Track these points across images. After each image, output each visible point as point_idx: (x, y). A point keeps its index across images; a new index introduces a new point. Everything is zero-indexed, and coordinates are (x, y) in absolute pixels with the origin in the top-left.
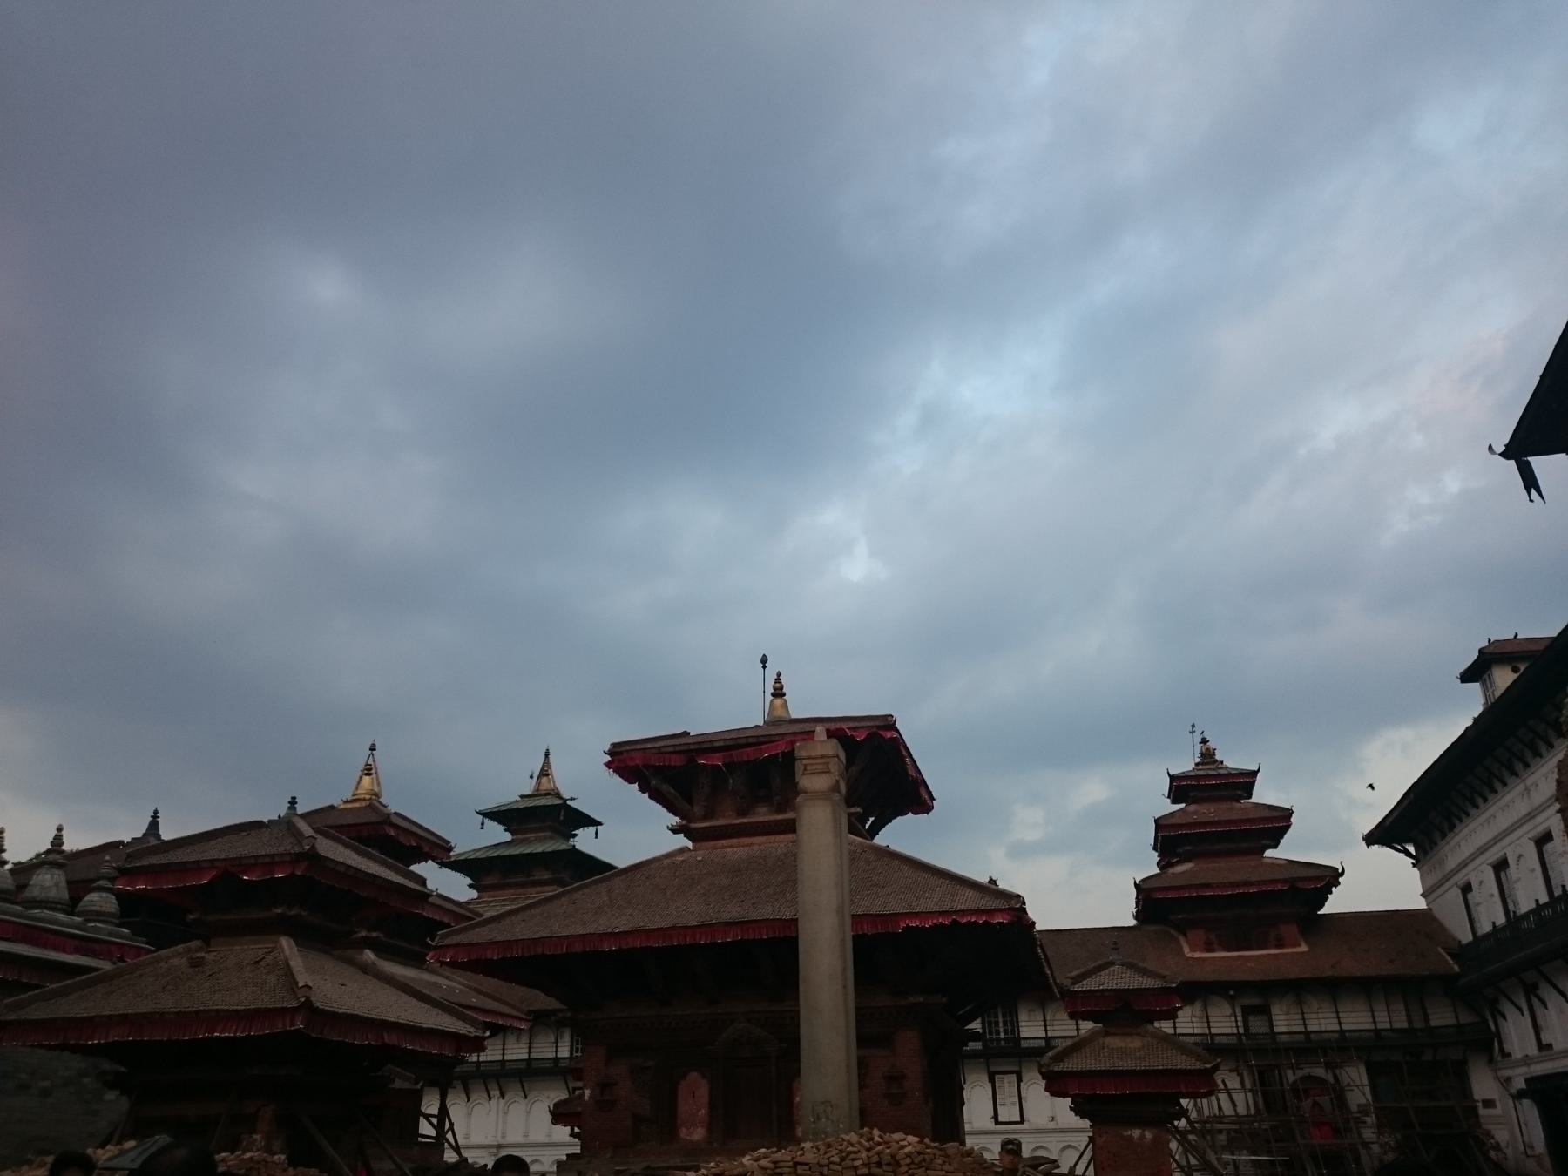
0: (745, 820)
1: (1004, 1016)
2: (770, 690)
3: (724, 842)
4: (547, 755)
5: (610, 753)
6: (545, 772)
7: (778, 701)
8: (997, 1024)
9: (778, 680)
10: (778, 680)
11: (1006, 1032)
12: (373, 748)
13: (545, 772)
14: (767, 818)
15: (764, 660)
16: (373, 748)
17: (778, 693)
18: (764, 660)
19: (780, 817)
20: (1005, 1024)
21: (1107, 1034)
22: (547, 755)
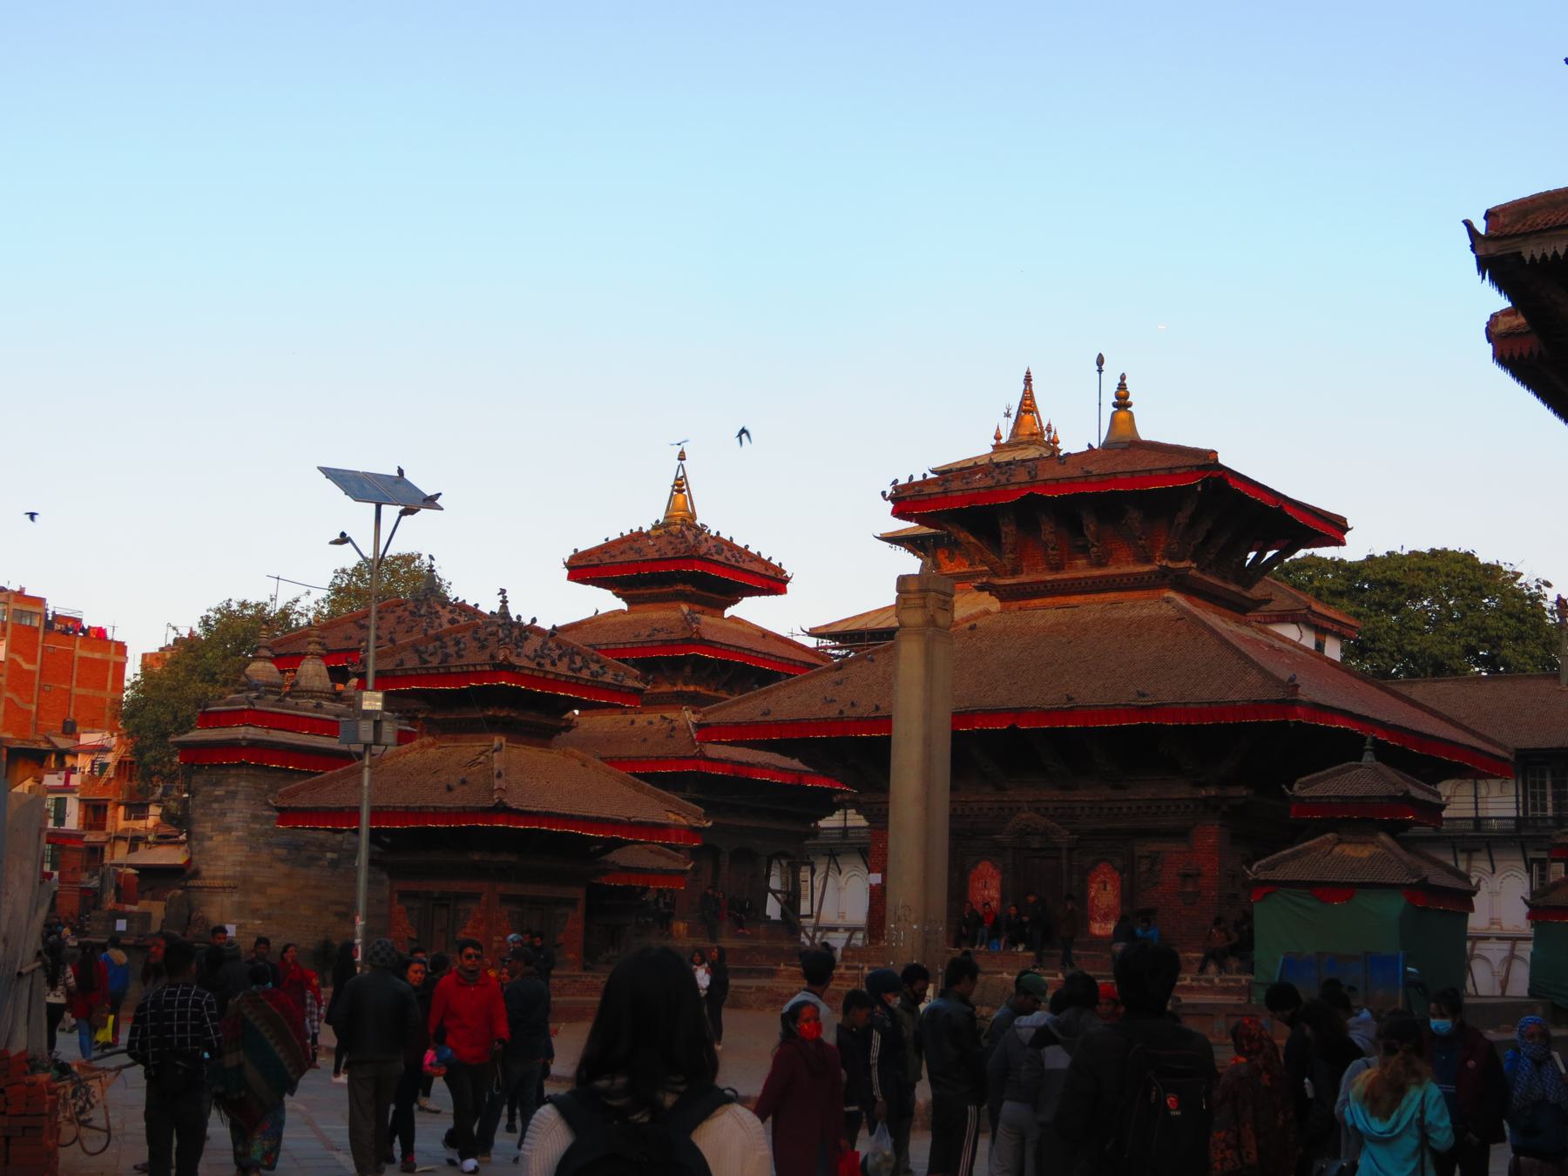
0: (1058, 576)
1: (1554, 785)
2: (1110, 398)
3: (1036, 602)
4: (1028, 379)
5: (893, 499)
6: (1028, 405)
7: (1122, 415)
8: (1544, 797)
9: (1122, 386)
10: (1122, 386)
11: (1556, 807)
12: (682, 457)
13: (1028, 405)
14: (1081, 574)
15: (1100, 361)
16: (682, 457)
17: (1122, 402)
18: (1100, 361)
19: (1097, 572)
20: (1554, 797)
21: (1340, 842)
22: (1028, 379)
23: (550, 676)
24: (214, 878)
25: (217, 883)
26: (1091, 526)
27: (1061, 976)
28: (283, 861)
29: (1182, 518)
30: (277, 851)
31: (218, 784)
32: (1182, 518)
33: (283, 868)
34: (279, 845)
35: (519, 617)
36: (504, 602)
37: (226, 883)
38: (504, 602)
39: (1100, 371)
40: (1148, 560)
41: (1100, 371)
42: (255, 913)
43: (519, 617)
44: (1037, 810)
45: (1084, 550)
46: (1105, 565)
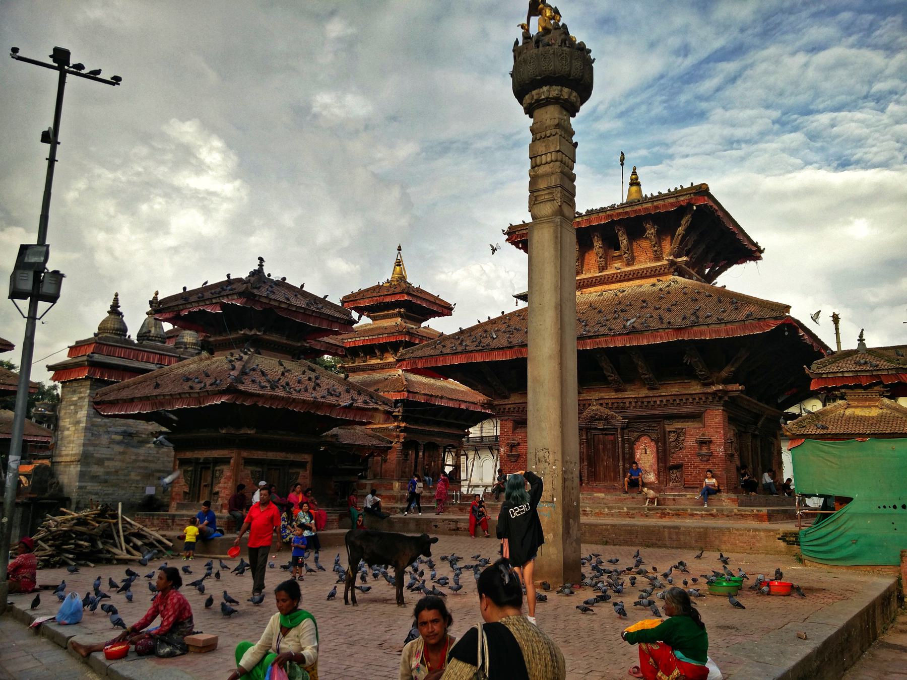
2: (627, 180)
5: (508, 233)
10: (634, 173)
23: (283, 306)
24: (67, 455)
25: (68, 459)
26: (624, 241)
27: (625, 509)
28: (120, 443)
29: (681, 230)
30: (114, 437)
31: (74, 392)
32: (681, 230)
33: (119, 448)
34: (116, 433)
35: (269, 275)
36: (261, 266)
37: (73, 458)
38: (261, 266)
39: (622, 164)
40: (658, 258)
41: (622, 164)
42: (94, 478)
43: (269, 275)
44: (601, 405)
45: (619, 257)
46: (633, 264)
